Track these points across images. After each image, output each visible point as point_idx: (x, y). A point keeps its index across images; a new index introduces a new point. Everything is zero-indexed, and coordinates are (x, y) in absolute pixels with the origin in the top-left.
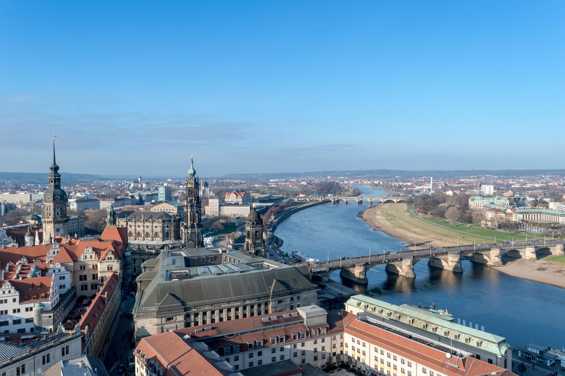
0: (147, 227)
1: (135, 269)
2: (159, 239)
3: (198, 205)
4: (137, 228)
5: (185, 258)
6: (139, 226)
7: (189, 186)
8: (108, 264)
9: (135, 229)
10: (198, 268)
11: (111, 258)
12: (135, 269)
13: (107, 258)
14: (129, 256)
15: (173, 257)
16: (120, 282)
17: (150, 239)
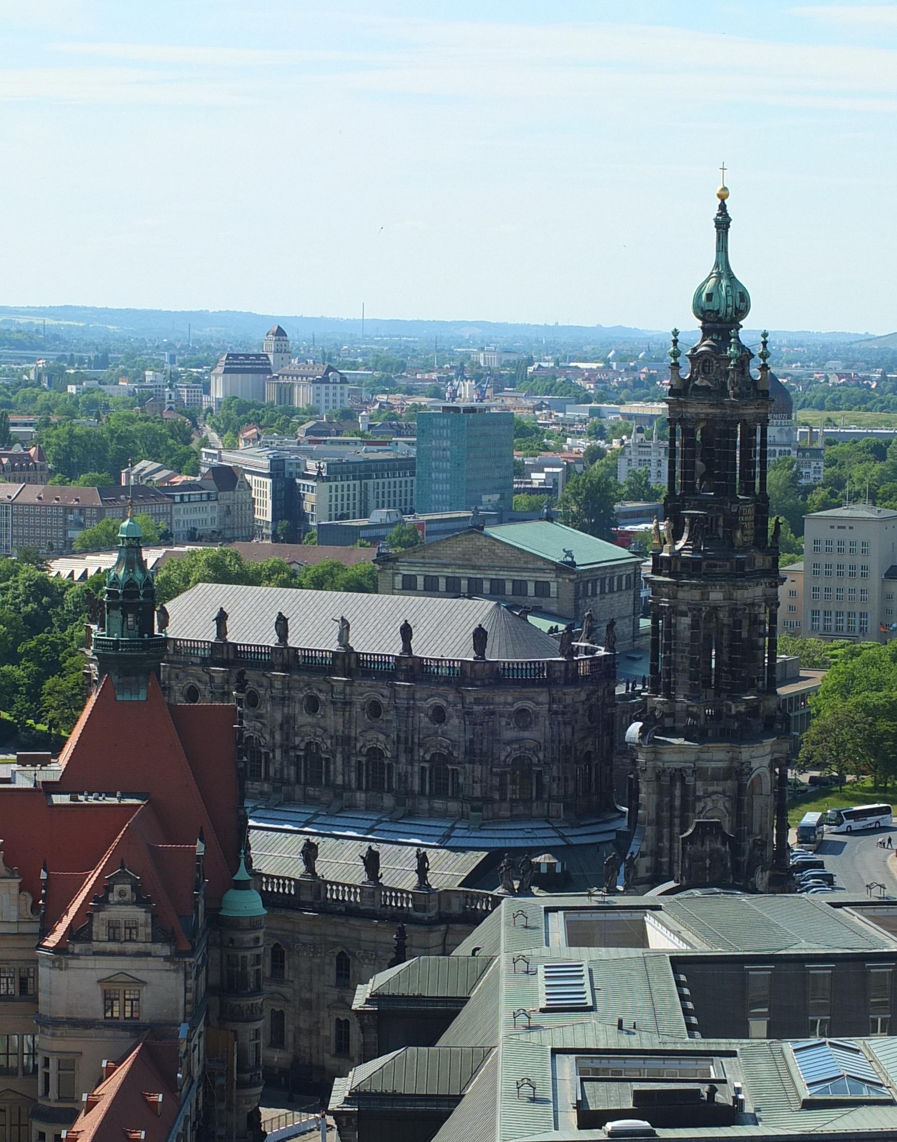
0: (375, 709)
1: (278, 1018)
2: (454, 806)
3: (761, 561)
4: (304, 718)
5: (678, 962)
6: (313, 705)
7: (698, 409)
8: (107, 967)
9: (288, 721)
10: (788, 1046)
11: (132, 927)
12: (278, 1018)
13: (99, 930)
14: (254, 924)
15: (586, 955)
16: (187, 1110)
17: (388, 801)
